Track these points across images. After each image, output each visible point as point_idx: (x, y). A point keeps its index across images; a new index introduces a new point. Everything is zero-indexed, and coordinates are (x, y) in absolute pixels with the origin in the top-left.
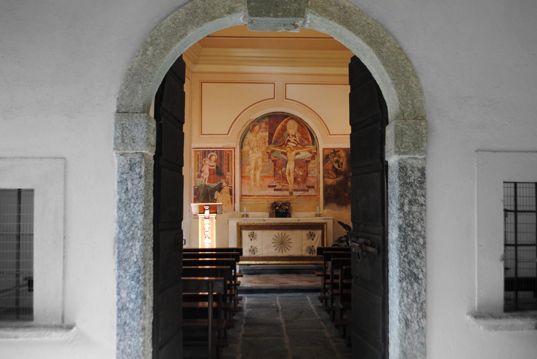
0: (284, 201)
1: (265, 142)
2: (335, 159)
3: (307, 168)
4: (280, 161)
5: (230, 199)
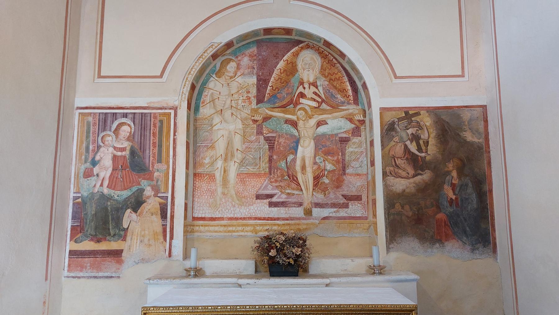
0: (291, 233)
1: (249, 98)
2: (410, 131)
3: (343, 154)
4: (282, 140)
5: (160, 229)
